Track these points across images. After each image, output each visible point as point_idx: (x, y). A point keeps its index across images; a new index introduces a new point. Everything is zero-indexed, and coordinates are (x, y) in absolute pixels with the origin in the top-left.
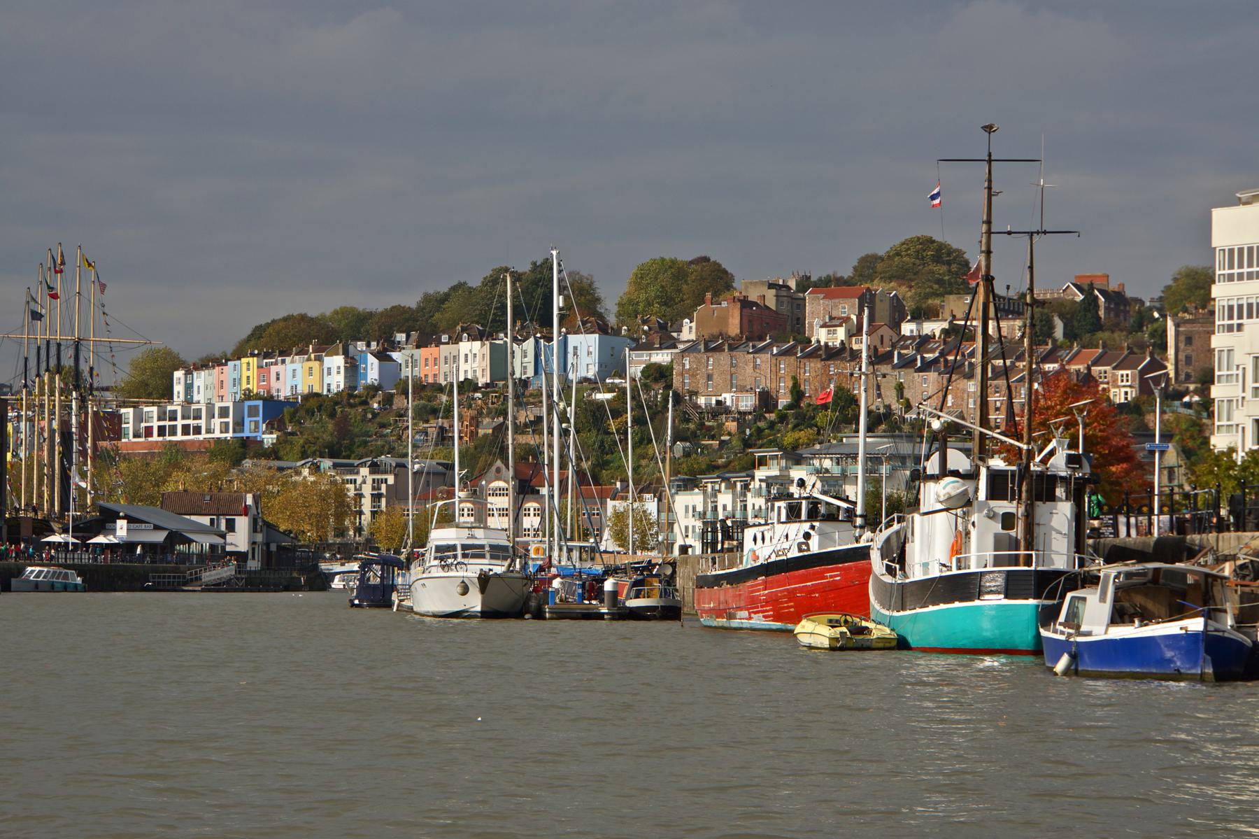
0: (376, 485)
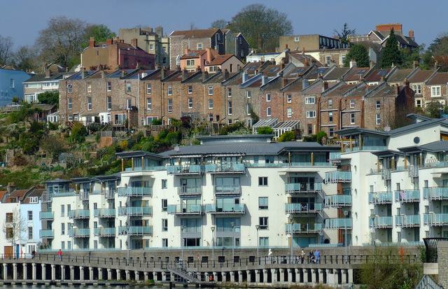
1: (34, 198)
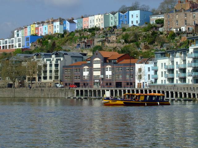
0: (57, 60)
1: (151, 62)
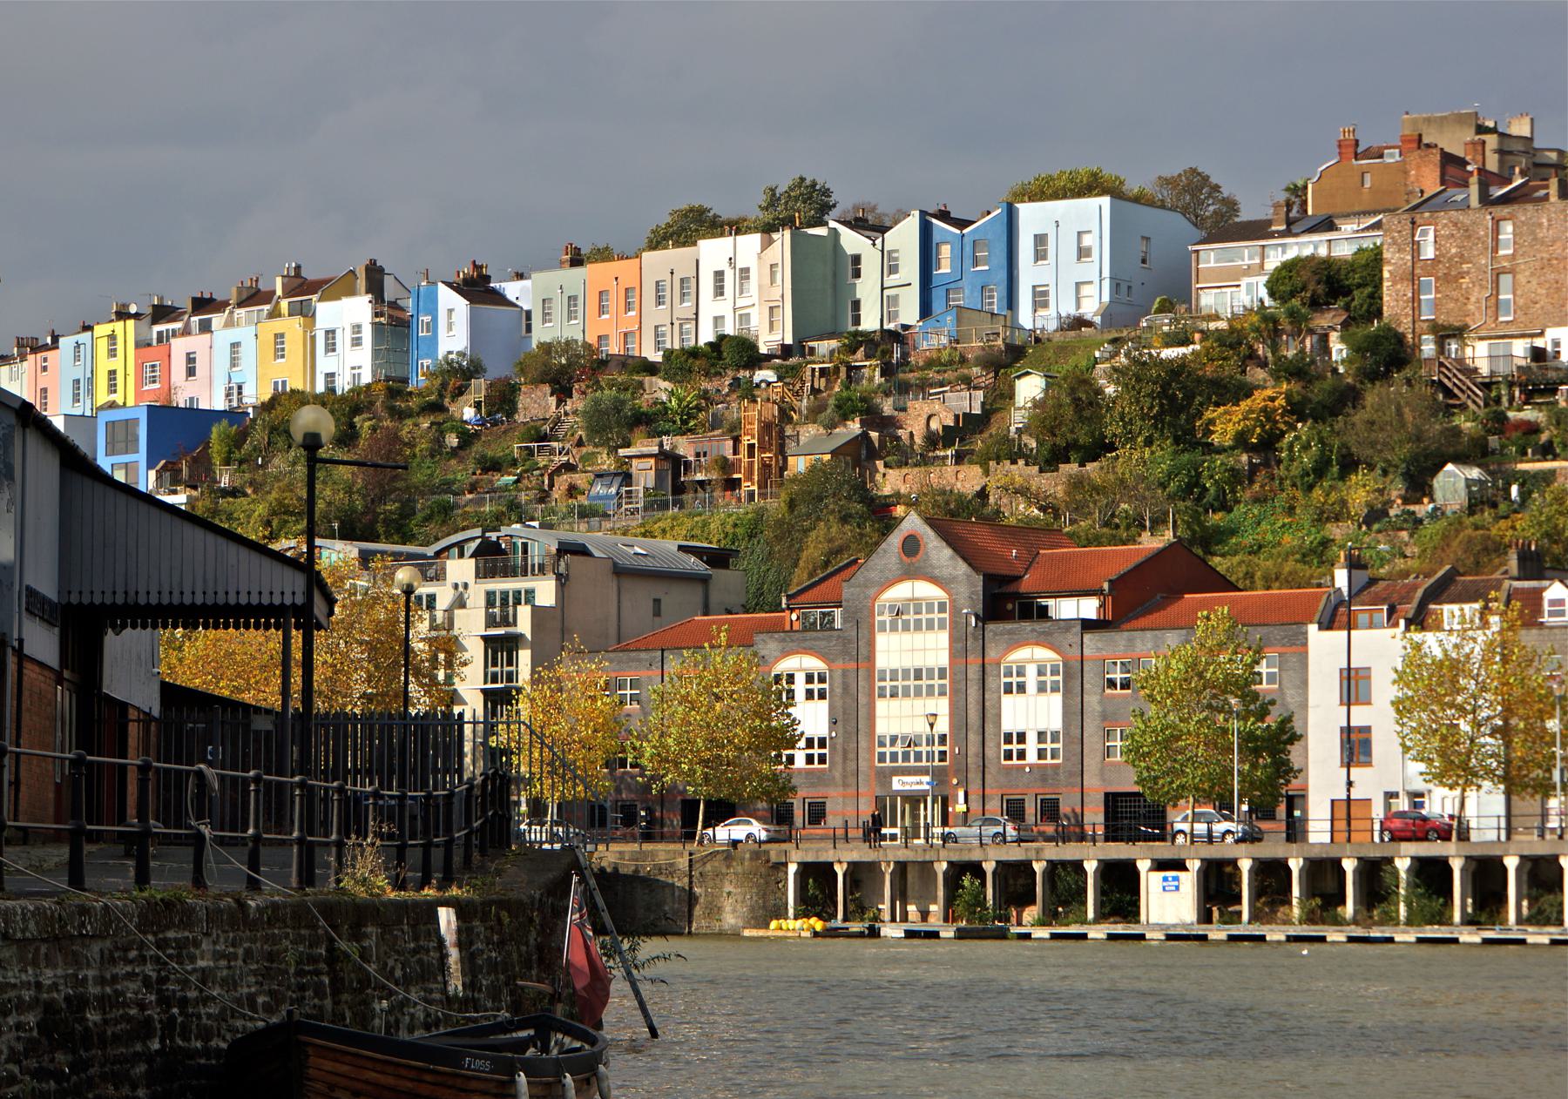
0: (500, 609)
